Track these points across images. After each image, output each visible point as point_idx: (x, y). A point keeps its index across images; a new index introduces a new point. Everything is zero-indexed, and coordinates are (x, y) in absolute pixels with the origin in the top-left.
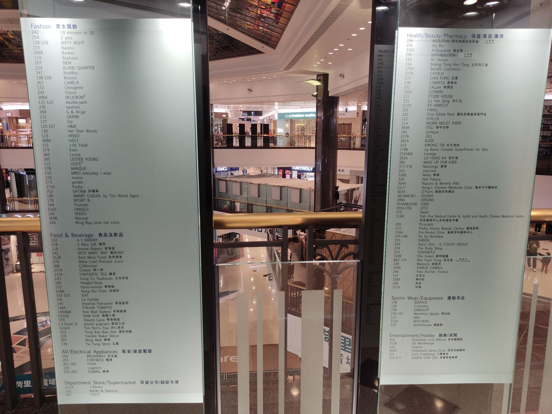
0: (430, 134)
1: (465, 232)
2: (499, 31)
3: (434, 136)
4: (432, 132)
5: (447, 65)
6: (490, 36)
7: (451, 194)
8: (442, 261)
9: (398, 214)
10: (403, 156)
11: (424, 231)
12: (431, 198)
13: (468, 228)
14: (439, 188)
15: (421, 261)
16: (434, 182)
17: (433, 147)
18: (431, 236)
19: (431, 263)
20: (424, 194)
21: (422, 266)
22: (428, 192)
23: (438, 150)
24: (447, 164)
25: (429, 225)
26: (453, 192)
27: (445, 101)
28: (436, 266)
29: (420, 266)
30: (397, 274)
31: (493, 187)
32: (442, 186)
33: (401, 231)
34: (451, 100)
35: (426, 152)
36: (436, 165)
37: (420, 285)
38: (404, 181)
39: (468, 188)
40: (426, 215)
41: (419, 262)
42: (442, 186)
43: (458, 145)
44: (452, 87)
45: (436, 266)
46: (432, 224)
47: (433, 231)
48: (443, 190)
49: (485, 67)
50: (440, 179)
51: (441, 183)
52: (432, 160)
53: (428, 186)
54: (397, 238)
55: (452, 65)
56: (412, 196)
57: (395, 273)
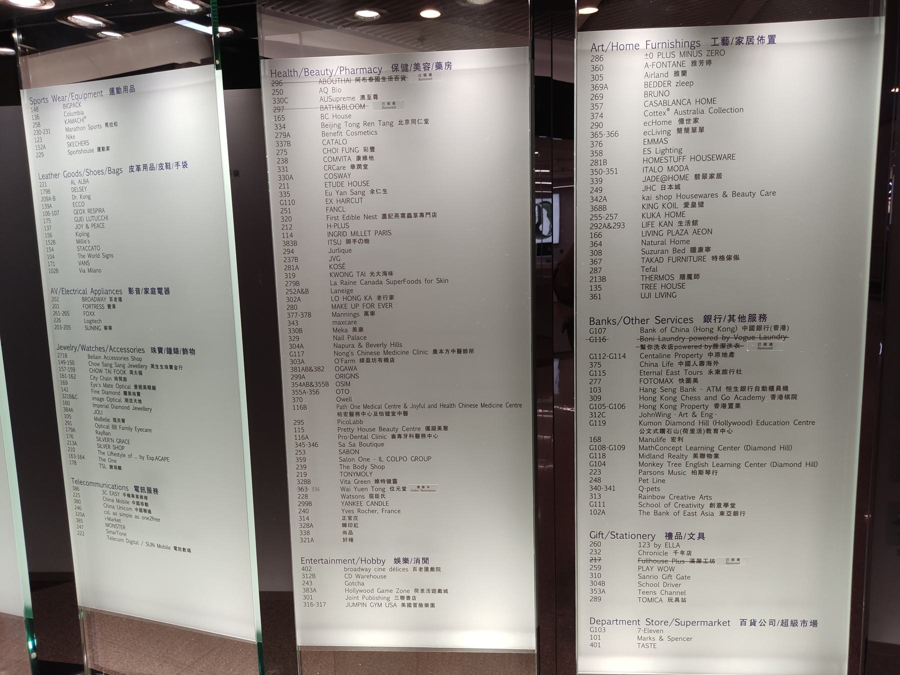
1: (423, 436)
2: (444, 56)
3: (344, 258)
5: (351, 125)
7: (389, 364)
9: (296, 404)
10: (293, 295)
11: (348, 434)
12: (353, 372)
13: (428, 428)
14: (366, 353)
15: (348, 490)
16: (356, 343)
17: (346, 279)
19: (366, 494)
20: (340, 365)
21: (351, 500)
22: (346, 362)
25: (354, 423)
26: (392, 360)
27: (356, 193)
28: (377, 500)
29: (348, 500)
30: (306, 515)
31: (465, 351)
32: (370, 350)
34: (367, 190)
35: (334, 288)
37: (350, 536)
38: (300, 342)
39: (419, 352)
40: (348, 404)
42: (370, 350)
44: (366, 166)
45: (377, 500)
46: (361, 422)
47: (364, 434)
48: (374, 357)
50: (365, 337)
51: (367, 344)
52: (345, 302)
53: (345, 350)
55: (361, 125)
56: (318, 369)
57: (302, 514)
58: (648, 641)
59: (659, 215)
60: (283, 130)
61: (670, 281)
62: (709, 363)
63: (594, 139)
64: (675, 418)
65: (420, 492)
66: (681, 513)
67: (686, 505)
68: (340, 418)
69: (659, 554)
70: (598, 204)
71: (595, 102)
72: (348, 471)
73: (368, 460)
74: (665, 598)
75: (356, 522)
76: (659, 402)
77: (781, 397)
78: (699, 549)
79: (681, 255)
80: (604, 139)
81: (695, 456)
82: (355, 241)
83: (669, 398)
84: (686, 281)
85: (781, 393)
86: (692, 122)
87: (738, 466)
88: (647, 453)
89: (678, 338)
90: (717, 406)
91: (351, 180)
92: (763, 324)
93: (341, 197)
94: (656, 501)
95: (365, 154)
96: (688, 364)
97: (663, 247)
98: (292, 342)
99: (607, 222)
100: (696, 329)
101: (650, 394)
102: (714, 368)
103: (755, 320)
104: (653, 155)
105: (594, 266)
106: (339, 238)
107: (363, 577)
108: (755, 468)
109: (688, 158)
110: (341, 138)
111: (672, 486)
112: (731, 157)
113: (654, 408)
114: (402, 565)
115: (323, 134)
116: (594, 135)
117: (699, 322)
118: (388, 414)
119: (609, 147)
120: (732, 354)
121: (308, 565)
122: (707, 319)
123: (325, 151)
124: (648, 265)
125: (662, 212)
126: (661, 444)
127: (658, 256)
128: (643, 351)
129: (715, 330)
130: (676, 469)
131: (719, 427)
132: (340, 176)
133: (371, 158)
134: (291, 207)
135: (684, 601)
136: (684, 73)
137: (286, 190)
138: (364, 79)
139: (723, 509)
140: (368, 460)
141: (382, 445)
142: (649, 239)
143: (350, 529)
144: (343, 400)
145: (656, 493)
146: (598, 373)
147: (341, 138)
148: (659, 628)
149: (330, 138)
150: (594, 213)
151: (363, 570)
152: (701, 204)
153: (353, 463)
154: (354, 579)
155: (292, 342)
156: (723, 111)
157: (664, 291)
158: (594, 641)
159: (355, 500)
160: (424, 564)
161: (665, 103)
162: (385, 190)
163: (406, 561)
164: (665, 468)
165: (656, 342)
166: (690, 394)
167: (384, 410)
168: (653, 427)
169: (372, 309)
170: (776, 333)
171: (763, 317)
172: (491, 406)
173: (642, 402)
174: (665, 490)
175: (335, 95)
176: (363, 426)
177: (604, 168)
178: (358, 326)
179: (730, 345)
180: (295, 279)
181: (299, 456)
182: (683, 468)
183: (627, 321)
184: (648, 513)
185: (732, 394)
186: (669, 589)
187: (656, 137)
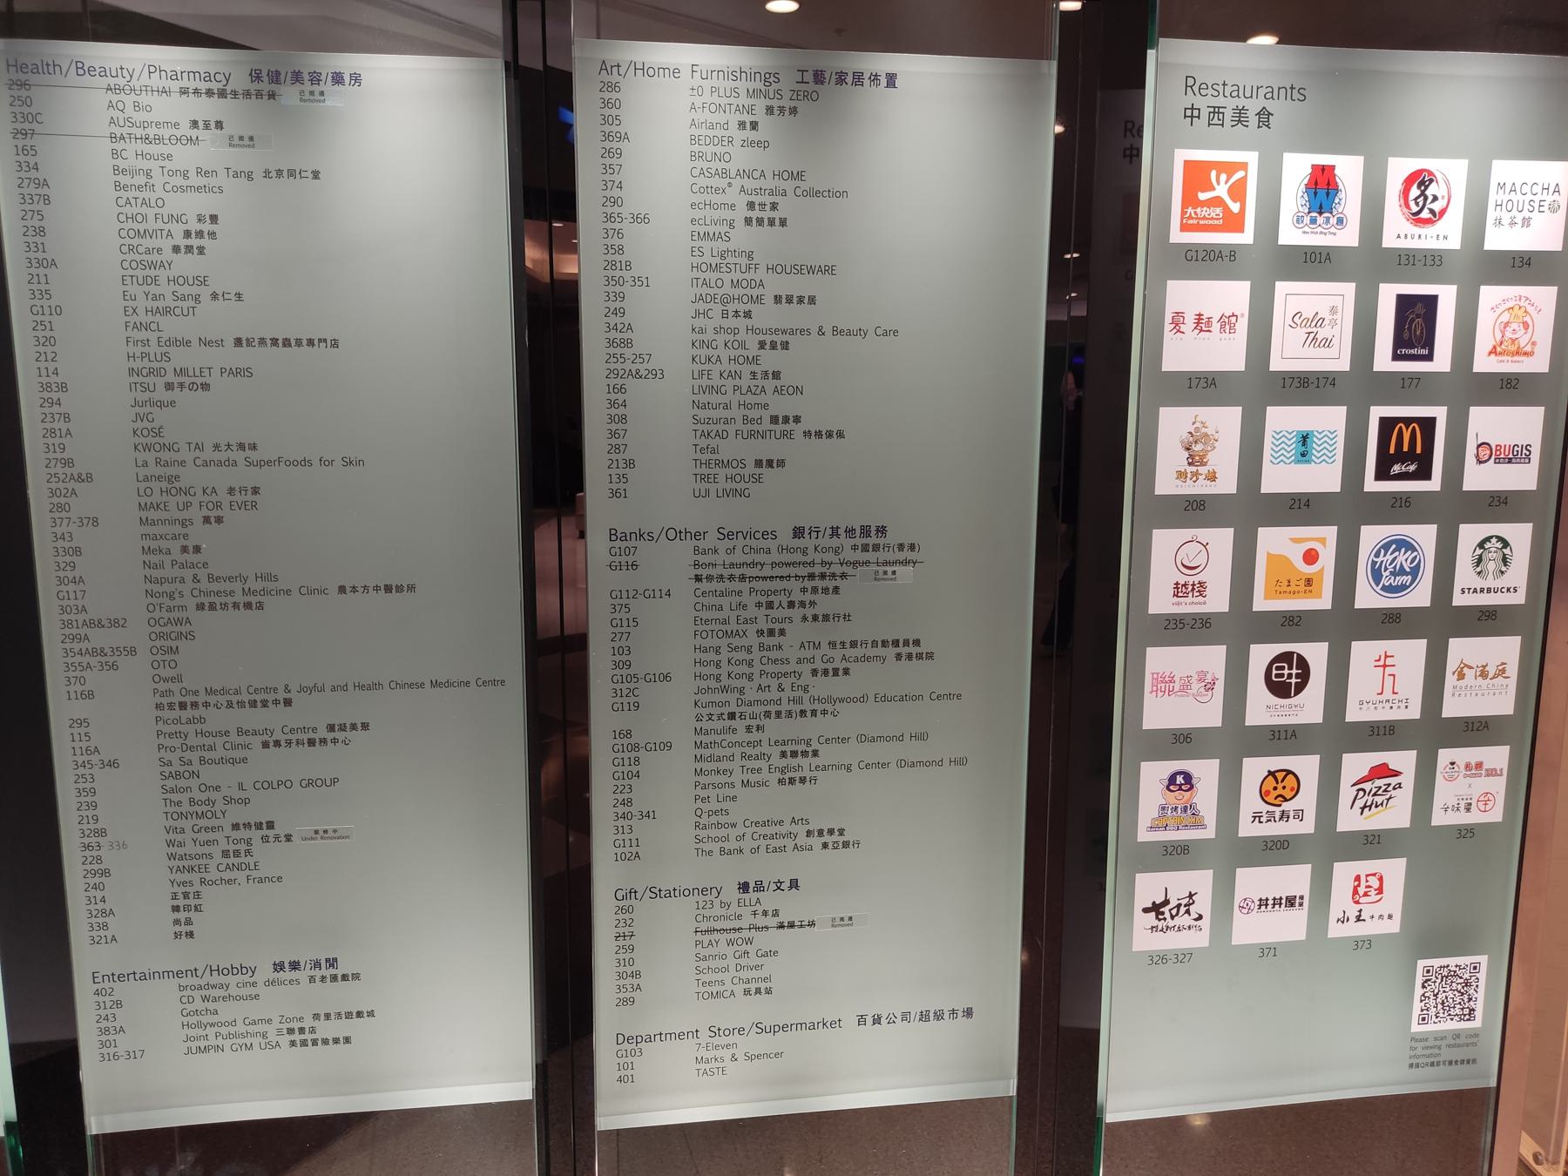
0: (148, 409)
1: (323, 741)
2: (349, 62)
3: (161, 417)
4: (153, 404)
5: (173, 173)
6: (315, 78)
7: (254, 613)
8: (257, 841)
9: (72, 689)
10: (61, 485)
11: (176, 742)
12: (184, 629)
13: (331, 728)
14: (208, 594)
15: (181, 845)
16: (188, 574)
17: (166, 455)
18: (202, 760)
19: (216, 851)
20: (157, 615)
22: (169, 610)
23: (182, 463)
24: (225, 512)
25: (189, 722)
26: (260, 606)
27: (183, 298)
28: (236, 861)
29: (181, 863)
30: (99, 895)
31: (399, 589)
32: (215, 587)
33: (92, 744)
34: (206, 293)
35: (143, 472)
36: (185, 515)
37: (188, 928)
38: (77, 574)
39: (311, 592)
40: (175, 687)
41: (172, 850)
42: (215, 587)
43: (254, 447)
44: (201, 250)
45: (236, 861)
46: (202, 720)
47: (208, 741)
48: (223, 600)
49: (311, 181)
50: (205, 565)
51: (211, 578)
52: (165, 498)
53: (167, 587)
54: (81, 771)
55: (192, 174)
56: (115, 623)
57: (93, 893)
58: (714, 1064)
59: (719, 359)
60: (33, 174)
61: (739, 470)
62: (802, 604)
63: (609, 225)
64: (751, 694)
65: (319, 841)
66: (763, 849)
67: (774, 835)
68: (159, 713)
69: (728, 918)
70: (619, 335)
71: (608, 161)
72: (178, 809)
73: (217, 788)
74: (739, 989)
75: (197, 902)
76: (725, 668)
77: (910, 657)
78: (791, 906)
79: (756, 427)
80: (626, 226)
81: (783, 754)
82: (181, 385)
83: (741, 662)
84: (764, 470)
85: (909, 649)
86: (768, 208)
87: (849, 769)
88: (707, 752)
89: (753, 564)
90: (814, 672)
91: (174, 273)
92: (881, 541)
93: (155, 304)
94: (722, 832)
95: (199, 227)
96: (770, 605)
97: (727, 414)
98: (61, 574)
99: (634, 368)
100: (781, 549)
101: (711, 656)
102: (809, 612)
103: (872, 535)
104: (707, 259)
105: (614, 441)
106: (151, 380)
107: (215, 1000)
108: (873, 771)
109: (762, 268)
110: (153, 197)
111: (750, 805)
112: (829, 270)
113: (718, 679)
114: (288, 975)
115: (117, 185)
116: (609, 218)
117: (785, 538)
118: (253, 704)
119: (636, 240)
120: (836, 589)
121: (107, 985)
122: (798, 532)
123: (122, 218)
124: (703, 442)
125: (725, 354)
126: (730, 738)
127: (720, 427)
128: (698, 585)
129: (811, 551)
130: (753, 778)
131: (819, 707)
132: (152, 265)
133: (212, 235)
134: (55, 318)
135: (769, 991)
136: (754, 125)
137: (43, 287)
138: (196, 92)
139: (827, 838)
140: (217, 788)
141: (244, 760)
142: (704, 398)
143: (186, 914)
144: (166, 680)
145: (722, 819)
146: (625, 623)
147: (153, 197)
148: (730, 1040)
149: (131, 194)
150: (612, 351)
151: (214, 987)
152: (785, 345)
153: (190, 795)
154: (199, 1005)
155: (61, 574)
156: (817, 194)
157: (730, 485)
158: (623, 1073)
159: (194, 862)
160: (330, 969)
161: (724, 173)
162: (239, 295)
163: (295, 966)
164: (737, 777)
165: (719, 570)
166: (774, 654)
167: (245, 697)
168: (716, 711)
169: (219, 513)
170: (901, 556)
171: (882, 530)
172: (449, 684)
173: (699, 669)
174: (737, 813)
175: (139, 117)
176: (205, 727)
177: (627, 275)
178: (190, 544)
179: (833, 575)
180: (65, 455)
181: (81, 786)
182: (765, 775)
183: (671, 534)
184: (710, 853)
185: (837, 654)
186: (745, 974)
187: (711, 229)
